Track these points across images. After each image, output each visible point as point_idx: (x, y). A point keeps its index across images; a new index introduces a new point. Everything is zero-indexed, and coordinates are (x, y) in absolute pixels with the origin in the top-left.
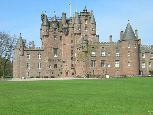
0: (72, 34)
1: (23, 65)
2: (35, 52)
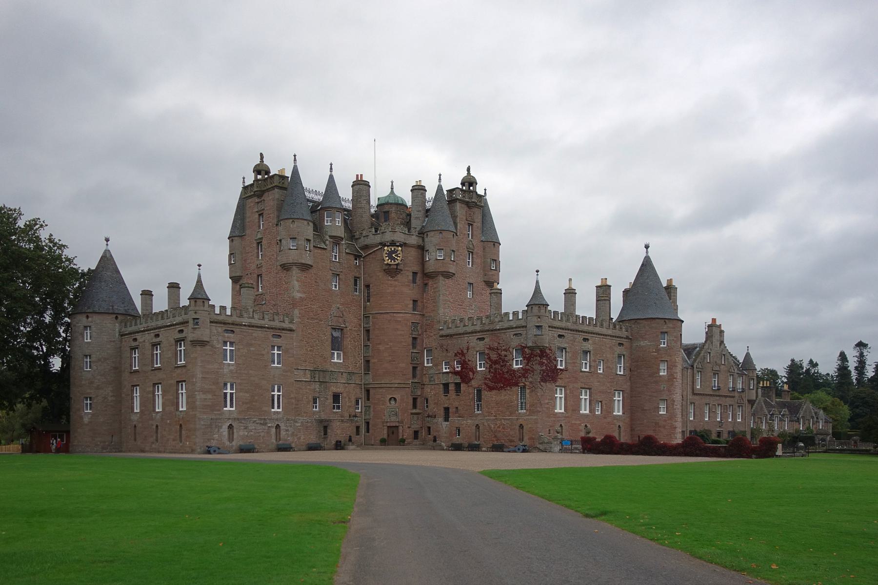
0: (415, 274)
1: (205, 392)
2: (258, 333)
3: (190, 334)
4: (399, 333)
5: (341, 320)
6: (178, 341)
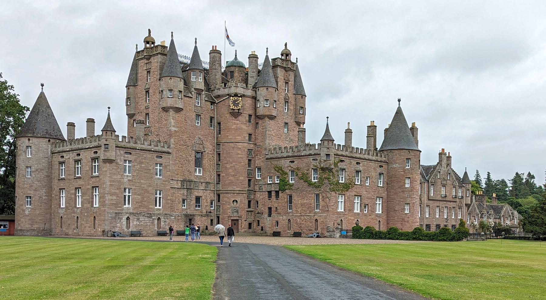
1: (112, 195)
2: (148, 155)
3: (101, 154)
4: (239, 156)
5: (201, 146)
6: (94, 159)
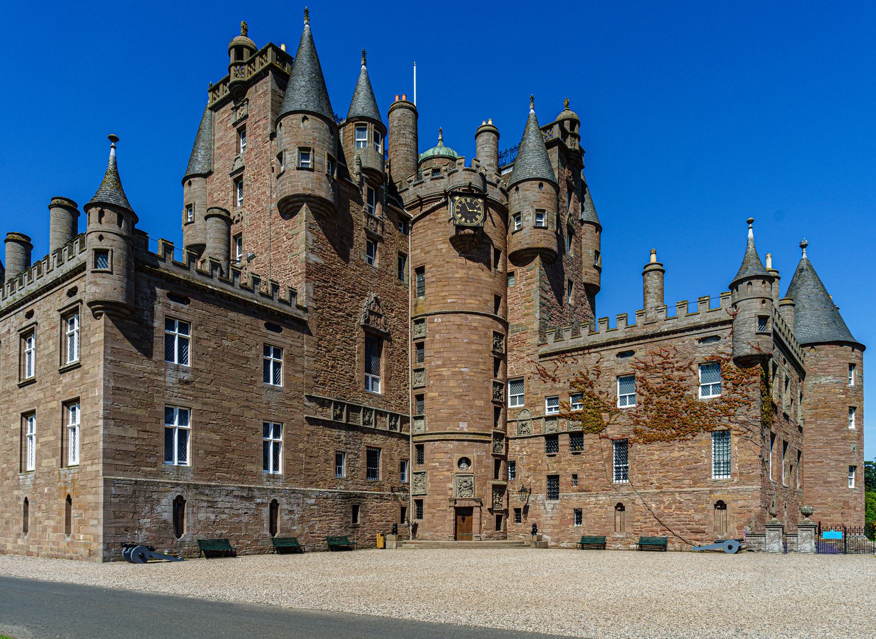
4: (474, 347)
